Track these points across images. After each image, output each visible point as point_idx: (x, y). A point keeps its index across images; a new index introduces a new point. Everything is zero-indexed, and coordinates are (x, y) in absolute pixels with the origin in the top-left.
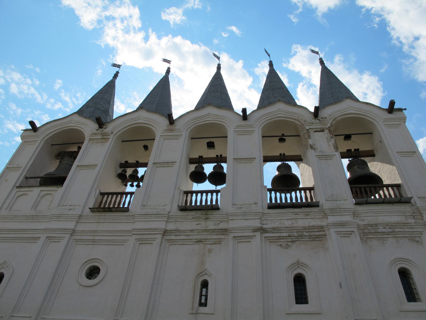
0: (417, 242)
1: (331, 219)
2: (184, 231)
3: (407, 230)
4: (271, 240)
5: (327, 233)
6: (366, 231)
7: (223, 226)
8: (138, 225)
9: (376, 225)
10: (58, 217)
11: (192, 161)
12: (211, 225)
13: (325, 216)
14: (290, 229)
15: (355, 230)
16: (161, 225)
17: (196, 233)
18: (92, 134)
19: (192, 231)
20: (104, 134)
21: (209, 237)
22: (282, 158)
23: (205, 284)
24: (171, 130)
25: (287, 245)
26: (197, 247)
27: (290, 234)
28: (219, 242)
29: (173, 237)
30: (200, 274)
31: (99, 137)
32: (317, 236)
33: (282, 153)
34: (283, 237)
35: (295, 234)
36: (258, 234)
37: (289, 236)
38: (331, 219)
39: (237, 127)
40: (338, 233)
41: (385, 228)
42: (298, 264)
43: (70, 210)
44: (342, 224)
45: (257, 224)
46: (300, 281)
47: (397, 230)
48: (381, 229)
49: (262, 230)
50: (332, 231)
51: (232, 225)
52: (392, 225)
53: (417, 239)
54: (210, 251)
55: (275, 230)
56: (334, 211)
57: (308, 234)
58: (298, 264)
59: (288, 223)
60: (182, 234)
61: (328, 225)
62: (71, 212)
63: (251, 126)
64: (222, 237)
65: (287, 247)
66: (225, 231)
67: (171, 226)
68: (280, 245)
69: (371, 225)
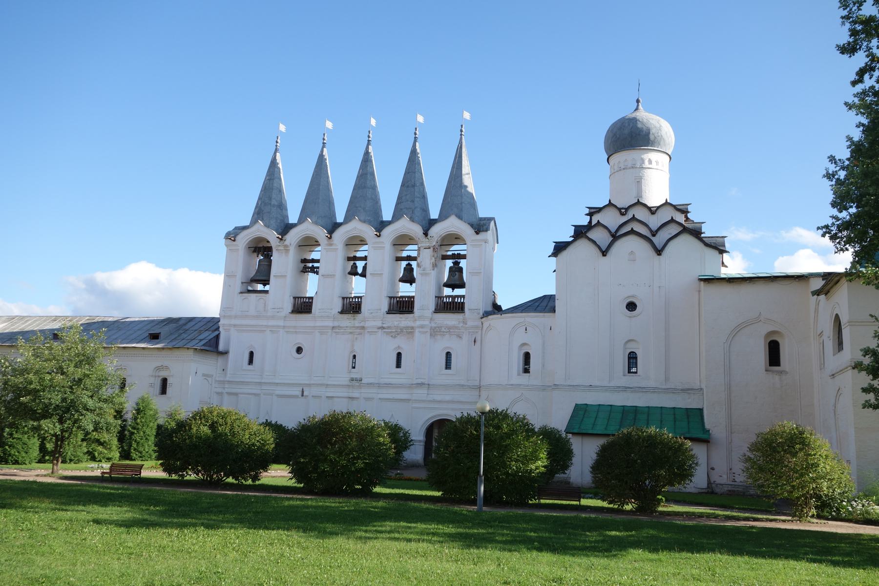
1: (418, 323)
4: (387, 333)
7: (362, 324)
8: (318, 324)
11: (349, 259)
12: (357, 324)
14: (397, 327)
20: (286, 246)
22: (409, 258)
23: (354, 357)
24: (331, 245)
28: (360, 334)
30: (352, 352)
32: (410, 332)
38: (418, 323)
44: (422, 327)
45: (379, 324)
46: (399, 355)
48: (443, 330)
49: (383, 328)
51: (367, 324)
52: (449, 328)
55: (389, 327)
56: (421, 317)
59: (396, 323)
62: (278, 314)
65: (395, 337)
66: (363, 328)
67: (336, 324)
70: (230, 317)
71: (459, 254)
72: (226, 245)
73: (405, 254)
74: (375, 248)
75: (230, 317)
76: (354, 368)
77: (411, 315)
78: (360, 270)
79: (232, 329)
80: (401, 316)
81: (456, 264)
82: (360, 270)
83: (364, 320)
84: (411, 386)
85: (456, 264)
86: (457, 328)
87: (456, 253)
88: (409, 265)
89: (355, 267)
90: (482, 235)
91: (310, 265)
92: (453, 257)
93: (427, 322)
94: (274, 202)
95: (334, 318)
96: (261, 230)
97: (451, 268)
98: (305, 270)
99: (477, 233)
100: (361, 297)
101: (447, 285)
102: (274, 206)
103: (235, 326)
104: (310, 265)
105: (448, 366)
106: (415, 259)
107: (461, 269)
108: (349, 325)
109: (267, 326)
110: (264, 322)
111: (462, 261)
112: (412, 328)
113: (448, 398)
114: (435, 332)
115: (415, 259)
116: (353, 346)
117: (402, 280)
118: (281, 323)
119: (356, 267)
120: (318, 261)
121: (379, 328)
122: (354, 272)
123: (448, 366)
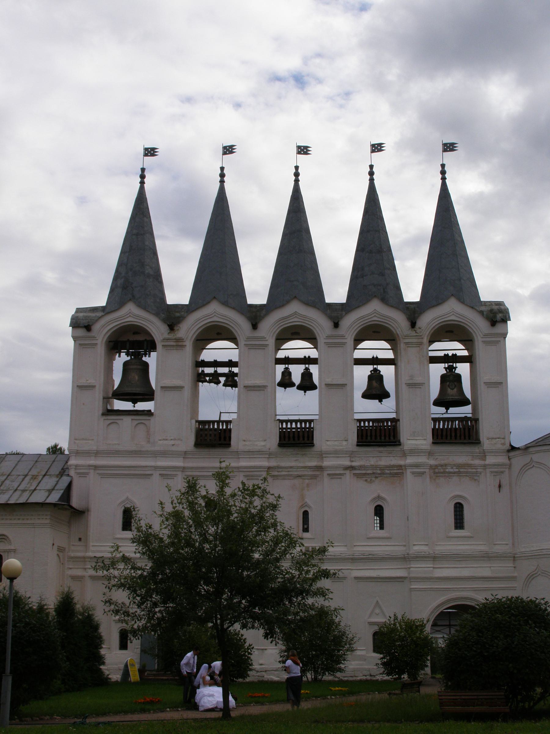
0: (475, 480)
1: (410, 460)
2: (286, 468)
3: (470, 470)
4: (358, 476)
5: (404, 472)
6: (437, 470)
9: (446, 465)
10: (164, 454)
13: (404, 455)
15: (427, 470)
16: (266, 464)
17: (295, 470)
18: (164, 339)
19: (291, 467)
21: (306, 473)
22: (375, 361)
23: (306, 514)
25: (371, 480)
26: (297, 482)
27: (375, 471)
28: (314, 477)
29: (276, 473)
30: (302, 506)
31: (172, 343)
33: (375, 356)
34: (368, 474)
35: (379, 472)
36: (348, 472)
37: (374, 473)
38: (410, 460)
39: (328, 337)
40: (413, 473)
41: (452, 468)
42: (379, 497)
43: (173, 445)
44: (417, 466)
45: (347, 463)
47: (461, 470)
48: (449, 469)
49: (352, 468)
50: (409, 471)
51: (326, 463)
52: (459, 466)
53: (476, 478)
54: (308, 485)
55: (361, 467)
57: (389, 472)
58: (379, 497)
59: (372, 462)
60: (284, 470)
61: (405, 466)
62: (174, 448)
63: (343, 337)
64: (318, 473)
65: (371, 482)
66: (320, 468)
67: (273, 463)
68: (366, 480)
69: (442, 466)
70: (87, 454)
71: (454, 356)
72: (75, 338)
73: (281, 354)
74: (330, 345)
75: (87, 454)
76: (306, 530)
77: (397, 449)
78: (297, 378)
79: (92, 471)
80: (381, 449)
81: (451, 369)
82: (297, 378)
83: (321, 455)
84: (406, 559)
85: (451, 369)
86: (469, 466)
87: (450, 353)
88: (375, 370)
89: (287, 374)
90: (499, 328)
91: (209, 370)
92: (445, 359)
93: (422, 459)
94: (148, 270)
95: (270, 455)
96: (131, 313)
97: (443, 377)
98: (201, 378)
99: (493, 323)
100: (310, 421)
101: (437, 403)
102: (149, 276)
103: (96, 467)
104: (209, 370)
105: (459, 523)
106: (314, 361)
107: (459, 377)
108: (293, 464)
109: (156, 468)
110: (150, 462)
111: (458, 365)
112: (400, 467)
113: (466, 573)
114: (438, 472)
115: (314, 361)
116: (302, 497)
117: (366, 395)
118: (179, 463)
119: (290, 374)
120: (235, 364)
121: (347, 468)
122: (286, 382)
123: (459, 523)
